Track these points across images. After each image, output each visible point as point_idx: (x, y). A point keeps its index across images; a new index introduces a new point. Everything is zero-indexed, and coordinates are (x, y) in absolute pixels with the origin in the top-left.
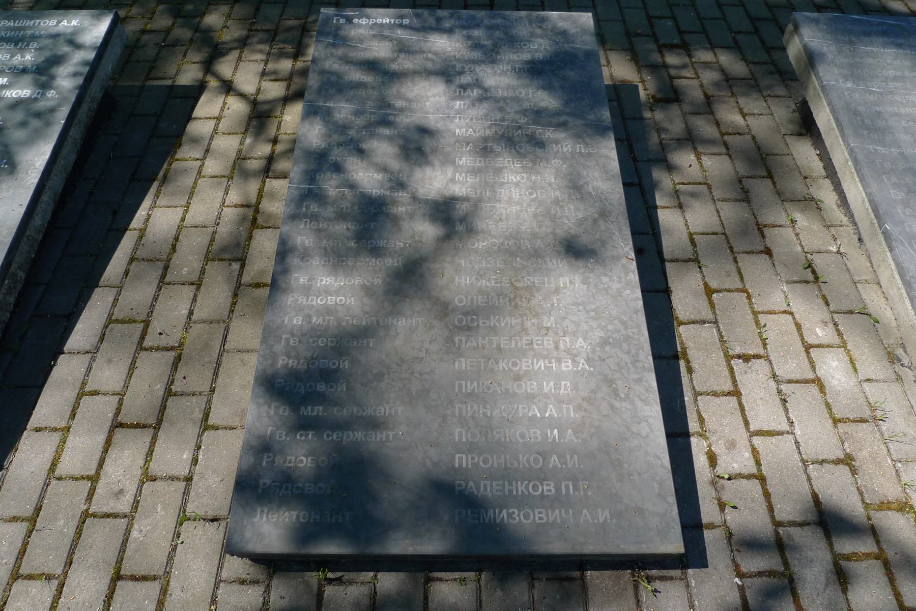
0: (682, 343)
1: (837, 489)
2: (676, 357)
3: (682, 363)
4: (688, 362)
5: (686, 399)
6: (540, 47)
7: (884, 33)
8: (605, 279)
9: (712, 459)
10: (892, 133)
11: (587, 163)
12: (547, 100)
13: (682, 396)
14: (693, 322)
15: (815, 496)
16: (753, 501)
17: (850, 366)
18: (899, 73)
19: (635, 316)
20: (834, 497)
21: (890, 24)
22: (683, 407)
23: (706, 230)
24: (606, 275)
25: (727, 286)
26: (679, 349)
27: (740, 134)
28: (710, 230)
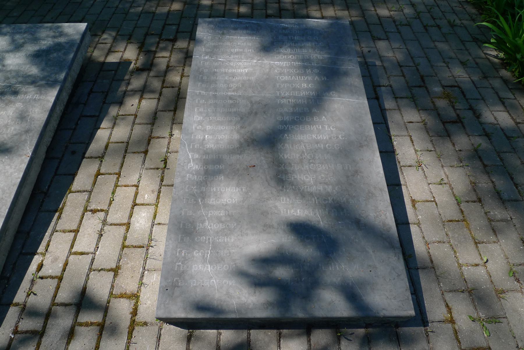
0: (65, 203)
1: (100, 287)
2: (56, 211)
3: (57, 214)
4: (61, 213)
5: (47, 234)
6: (46, 43)
7: (246, 28)
8: (7, 167)
9: (40, 267)
10: (216, 84)
11: (35, 105)
12: (34, 70)
13: (46, 232)
14: (78, 192)
15: (84, 289)
16: (47, 291)
17: (152, 216)
18: (241, 50)
19: (12, 187)
20: (95, 290)
21: (253, 23)
22: (42, 239)
23: (118, 141)
24: (9, 165)
25: (110, 172)
26: (60, 207)
27: (173, 87)
28: (121, 141)
